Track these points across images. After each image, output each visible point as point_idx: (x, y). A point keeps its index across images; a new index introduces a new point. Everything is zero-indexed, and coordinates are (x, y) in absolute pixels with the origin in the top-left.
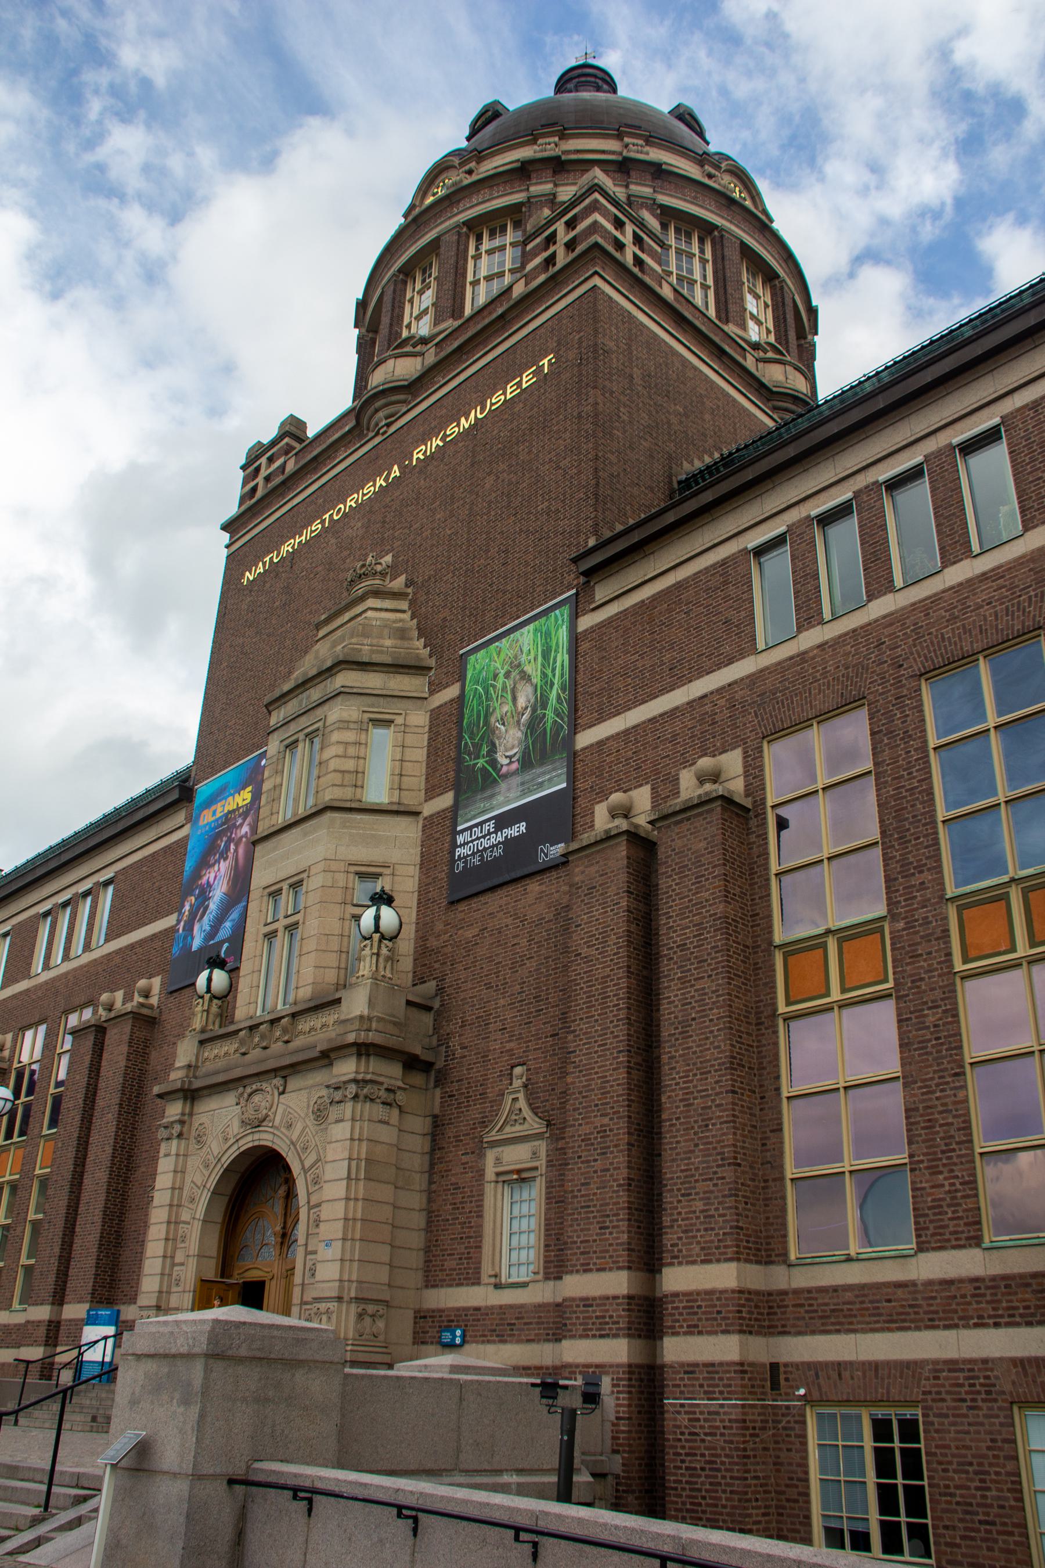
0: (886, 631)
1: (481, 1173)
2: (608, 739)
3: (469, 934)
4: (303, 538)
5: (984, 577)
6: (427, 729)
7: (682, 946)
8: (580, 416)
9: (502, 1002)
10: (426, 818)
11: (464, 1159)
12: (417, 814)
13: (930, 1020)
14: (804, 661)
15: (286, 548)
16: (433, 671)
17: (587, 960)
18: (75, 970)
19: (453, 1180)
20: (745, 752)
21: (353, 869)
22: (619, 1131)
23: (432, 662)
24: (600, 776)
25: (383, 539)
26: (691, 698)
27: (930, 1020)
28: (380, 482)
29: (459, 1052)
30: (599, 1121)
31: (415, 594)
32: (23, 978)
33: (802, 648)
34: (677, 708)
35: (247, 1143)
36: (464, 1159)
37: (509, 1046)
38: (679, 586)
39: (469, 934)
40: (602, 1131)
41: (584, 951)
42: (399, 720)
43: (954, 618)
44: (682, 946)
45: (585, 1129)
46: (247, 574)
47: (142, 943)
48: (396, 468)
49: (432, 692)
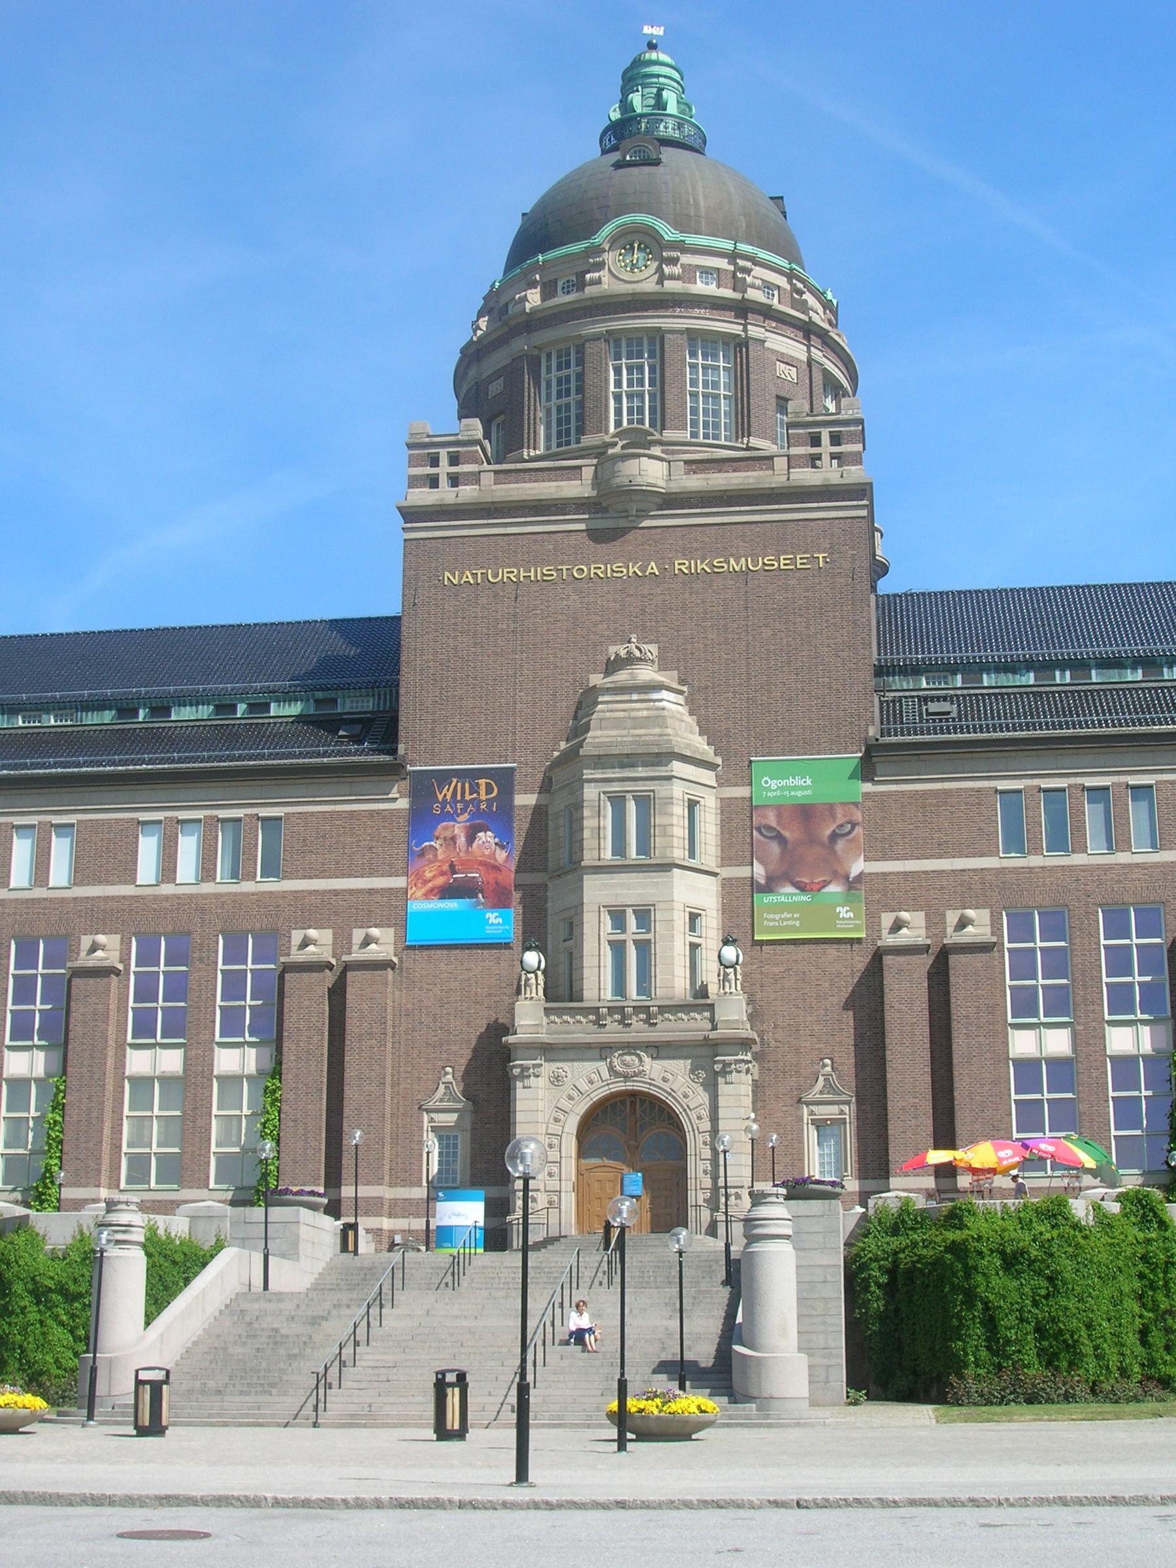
0: (1082, 874)
1: (800, 1119)
2: (890, 873)
3: (776, 970)
4: (532, 574)
5: (1137, 865)
6: (719, 811)
7: (967, 1017)
8: (855, 622)
9: (809, 1018)
10: (724, 879)
11: (784, 1109)
12: (715, 874)
13: (1094, 1075)
14: (1031, 872)
15: (504, 574)
16: (720, 768)
17: (899, 1011)
18: (235, 894)
19: (776, 1120)
20: (992, 913)
21: (688, 910)
22: (926, 1106)
23: (719, 760)
24: (885, 895)
25: (644, 627)
26: (954, 868)
27: (1094, 1075)
28: (634, 569)
29: (773, 1043)
30: (912, 1101)
31: (691, 694)
32: (125, 882)
33: (1031, 865)
34: (943, 871)
35: (619, 1086)
36: (784, 1109)
37: (817, 1046)
38: (946, 792)
39: (776, 970)
40: (914, 1106)
41: (897, 1006)
42: (702, 802)
43: (1119, 882)
44: (967, 1017)
45: (900, 1104)
46: (447, 574)
47: (351, 892)
48: (653, 564)
49: (720, 785)
